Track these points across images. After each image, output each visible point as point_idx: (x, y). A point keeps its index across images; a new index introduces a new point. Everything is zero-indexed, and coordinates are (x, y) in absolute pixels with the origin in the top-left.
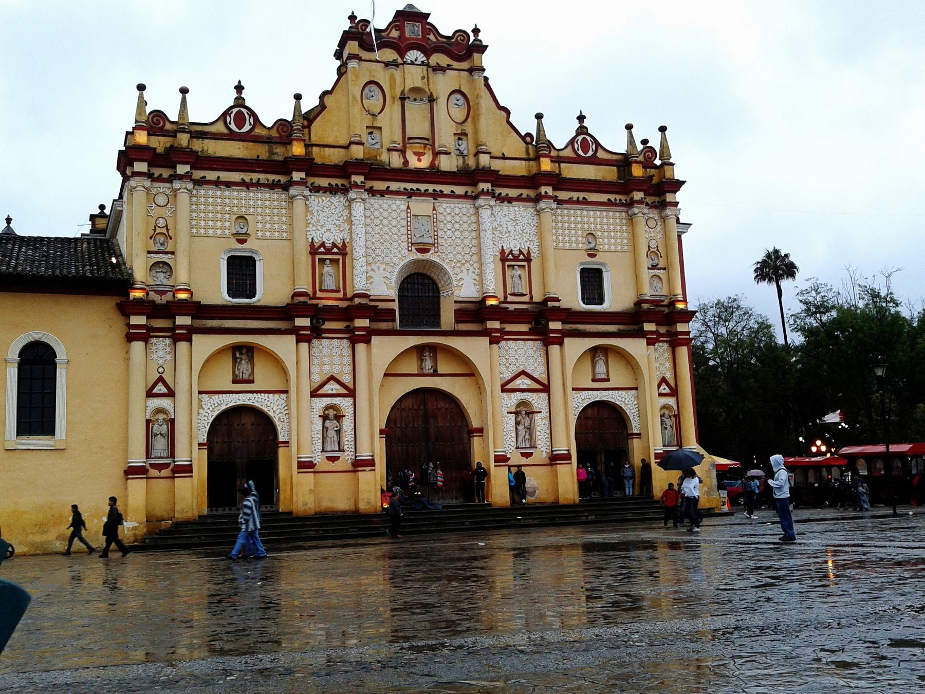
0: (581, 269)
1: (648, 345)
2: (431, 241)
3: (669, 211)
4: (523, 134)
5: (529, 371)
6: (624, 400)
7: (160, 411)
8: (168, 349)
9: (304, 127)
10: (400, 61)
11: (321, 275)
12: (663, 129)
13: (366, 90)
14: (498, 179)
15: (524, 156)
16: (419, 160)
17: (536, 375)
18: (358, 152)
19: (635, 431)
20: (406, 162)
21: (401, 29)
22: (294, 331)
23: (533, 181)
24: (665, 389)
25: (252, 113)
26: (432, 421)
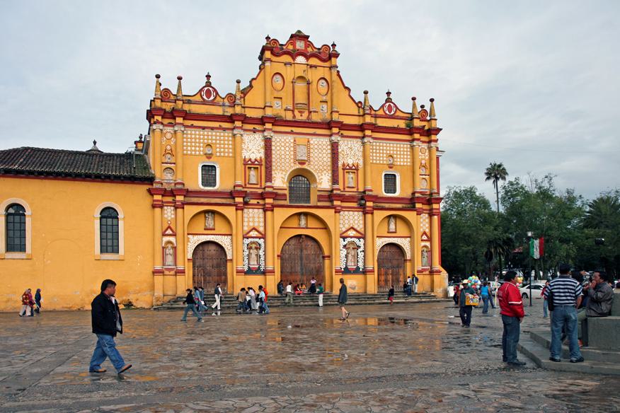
0: (385, 175)
2: (306, 159)
3: (433, 144)
4: (357, 102)
5: (356, 227)
6: (405, 243)
7: (169, 242)
8: (173, 212)
9: (241, 98)
10: (292, 61)
11: (249, 175)
12: (432, 100)
13: (274, 78)
14: (342, 126)
15: (357, 114)
16: (301, 116)
17: (358, 229)
18: (269, 112)
19: (408, 258)
20: (294, 116)
21: (294, 45)
22: (235, 205)
23: (361, 128)
24: (425, 237)
25: (215, 90)
26: (304, 251)
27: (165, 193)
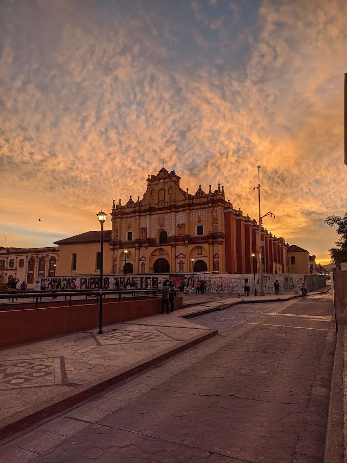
0: (198, 227)
1: (209, 245)
14: (176, 207)
22: (135, 247)
23: (183, 206)
27: (114, 244)
